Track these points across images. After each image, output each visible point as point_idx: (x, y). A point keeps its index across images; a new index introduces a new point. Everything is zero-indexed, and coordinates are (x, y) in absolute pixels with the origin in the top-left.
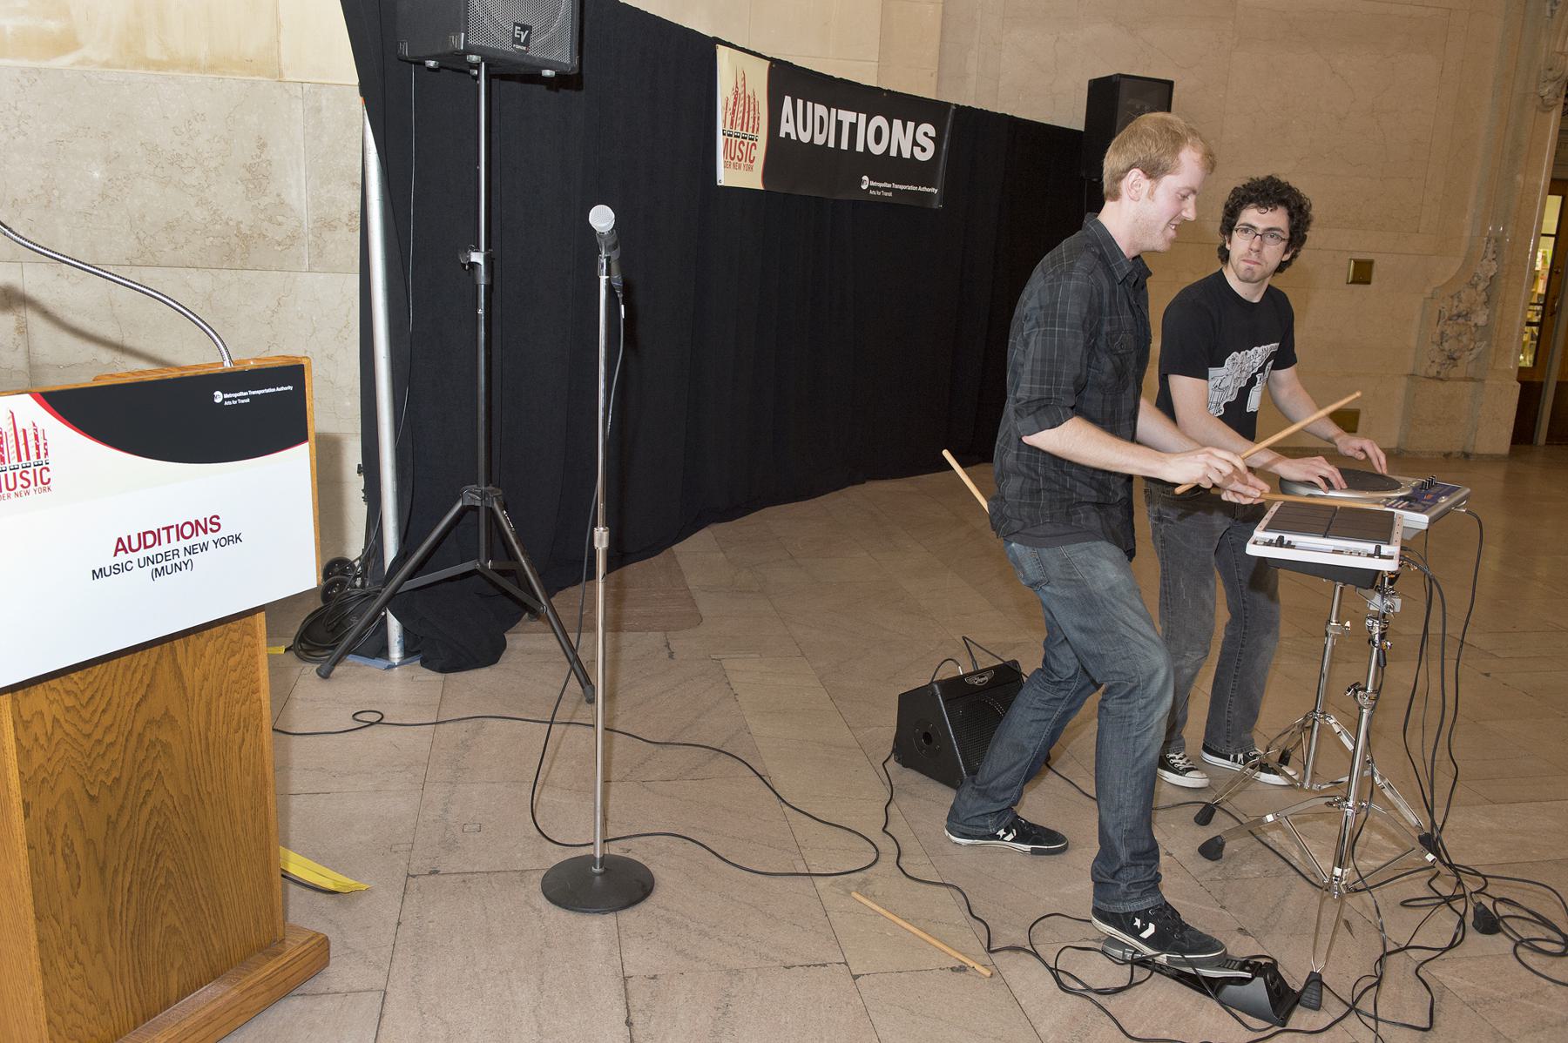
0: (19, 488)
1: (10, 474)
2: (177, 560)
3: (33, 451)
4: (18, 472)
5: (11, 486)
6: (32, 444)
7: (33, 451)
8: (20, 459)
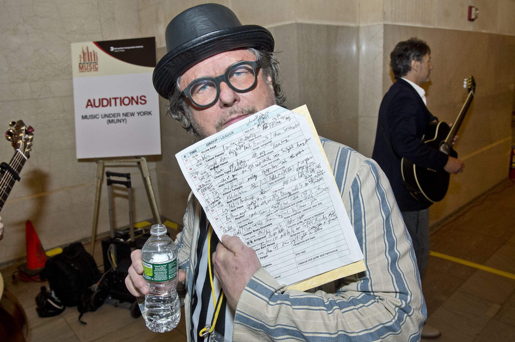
1: (86, 65)
2: (119, 118)
3: (93, 59)
6: (93, 56)
7: (93, 59)
8: (89, 60)
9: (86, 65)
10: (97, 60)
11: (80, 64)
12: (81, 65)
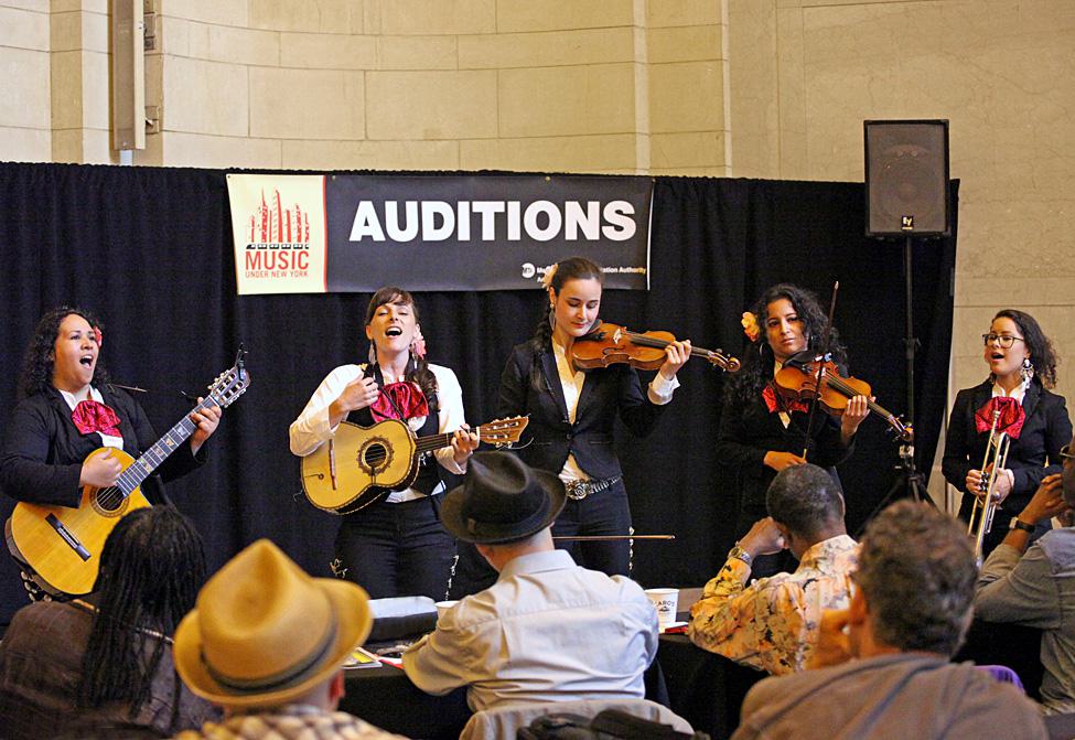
0: (276, 269)
3: (294, 234)
4: (277, 252)
5: (270, 265)
7: (294, 234)
8: (281, 240)
9: (270, 252)
10: (307, 238)
11: (249, 247)
12: (253, 252)
